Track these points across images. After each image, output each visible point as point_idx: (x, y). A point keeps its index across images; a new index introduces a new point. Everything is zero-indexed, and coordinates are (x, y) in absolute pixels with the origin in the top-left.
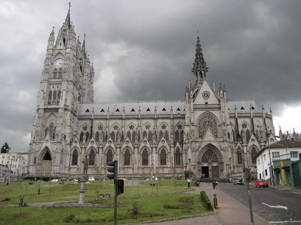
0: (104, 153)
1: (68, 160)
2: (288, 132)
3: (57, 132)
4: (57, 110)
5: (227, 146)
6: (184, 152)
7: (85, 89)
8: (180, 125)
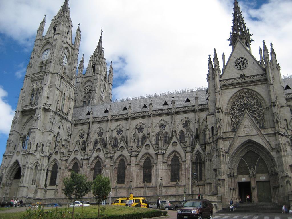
0: (90, 167)
1: (42, 178)
7: (95, 90)
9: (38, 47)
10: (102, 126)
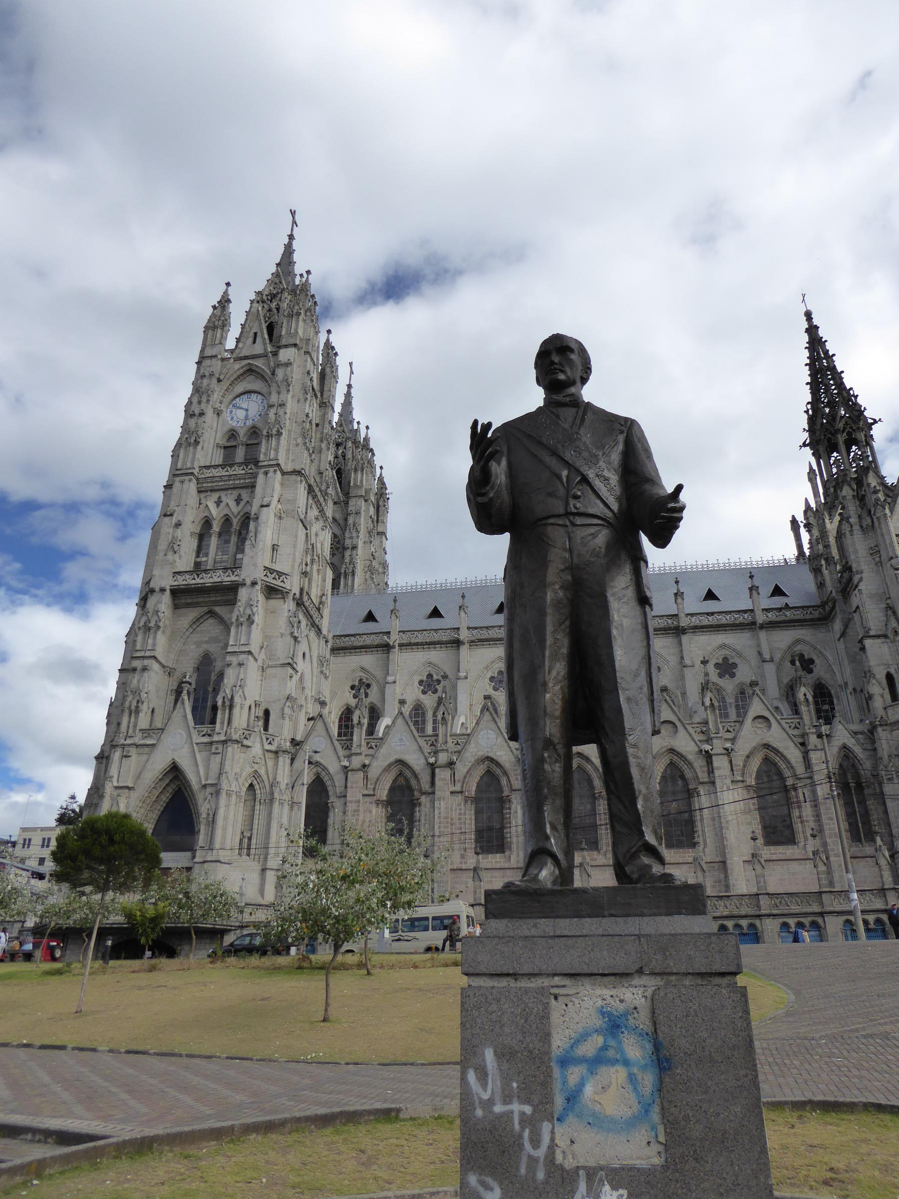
0: (461, 792)
7: (354, 548)
9: (215, 381)
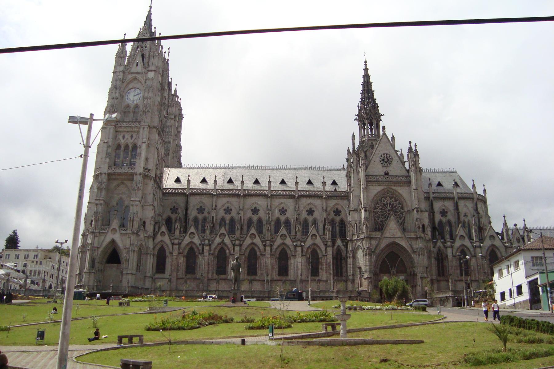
0: (212, 254)
1: (150, 263)
2: (515, 225)
3: (130, 215)
4: (131, 177)
5: (423, 247)
6: (351, 255)
8: (337, 209)
10: (204, 201)
